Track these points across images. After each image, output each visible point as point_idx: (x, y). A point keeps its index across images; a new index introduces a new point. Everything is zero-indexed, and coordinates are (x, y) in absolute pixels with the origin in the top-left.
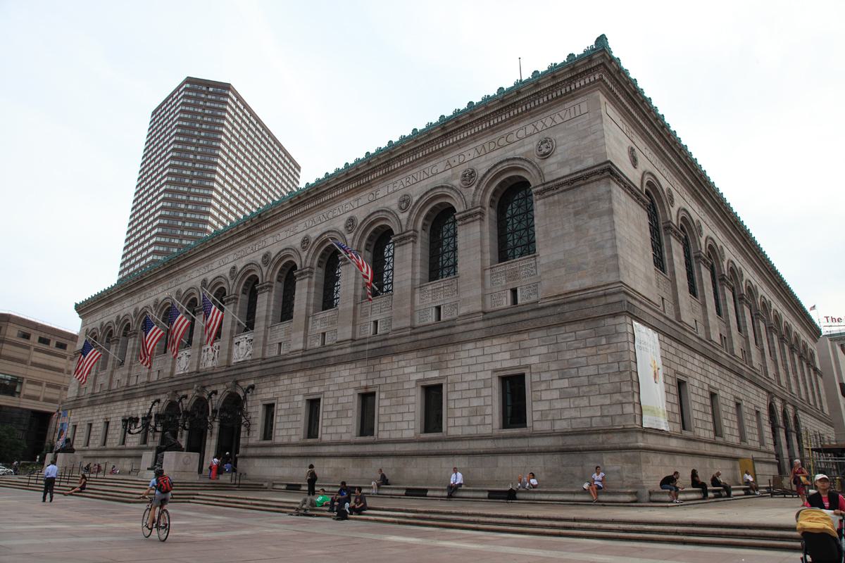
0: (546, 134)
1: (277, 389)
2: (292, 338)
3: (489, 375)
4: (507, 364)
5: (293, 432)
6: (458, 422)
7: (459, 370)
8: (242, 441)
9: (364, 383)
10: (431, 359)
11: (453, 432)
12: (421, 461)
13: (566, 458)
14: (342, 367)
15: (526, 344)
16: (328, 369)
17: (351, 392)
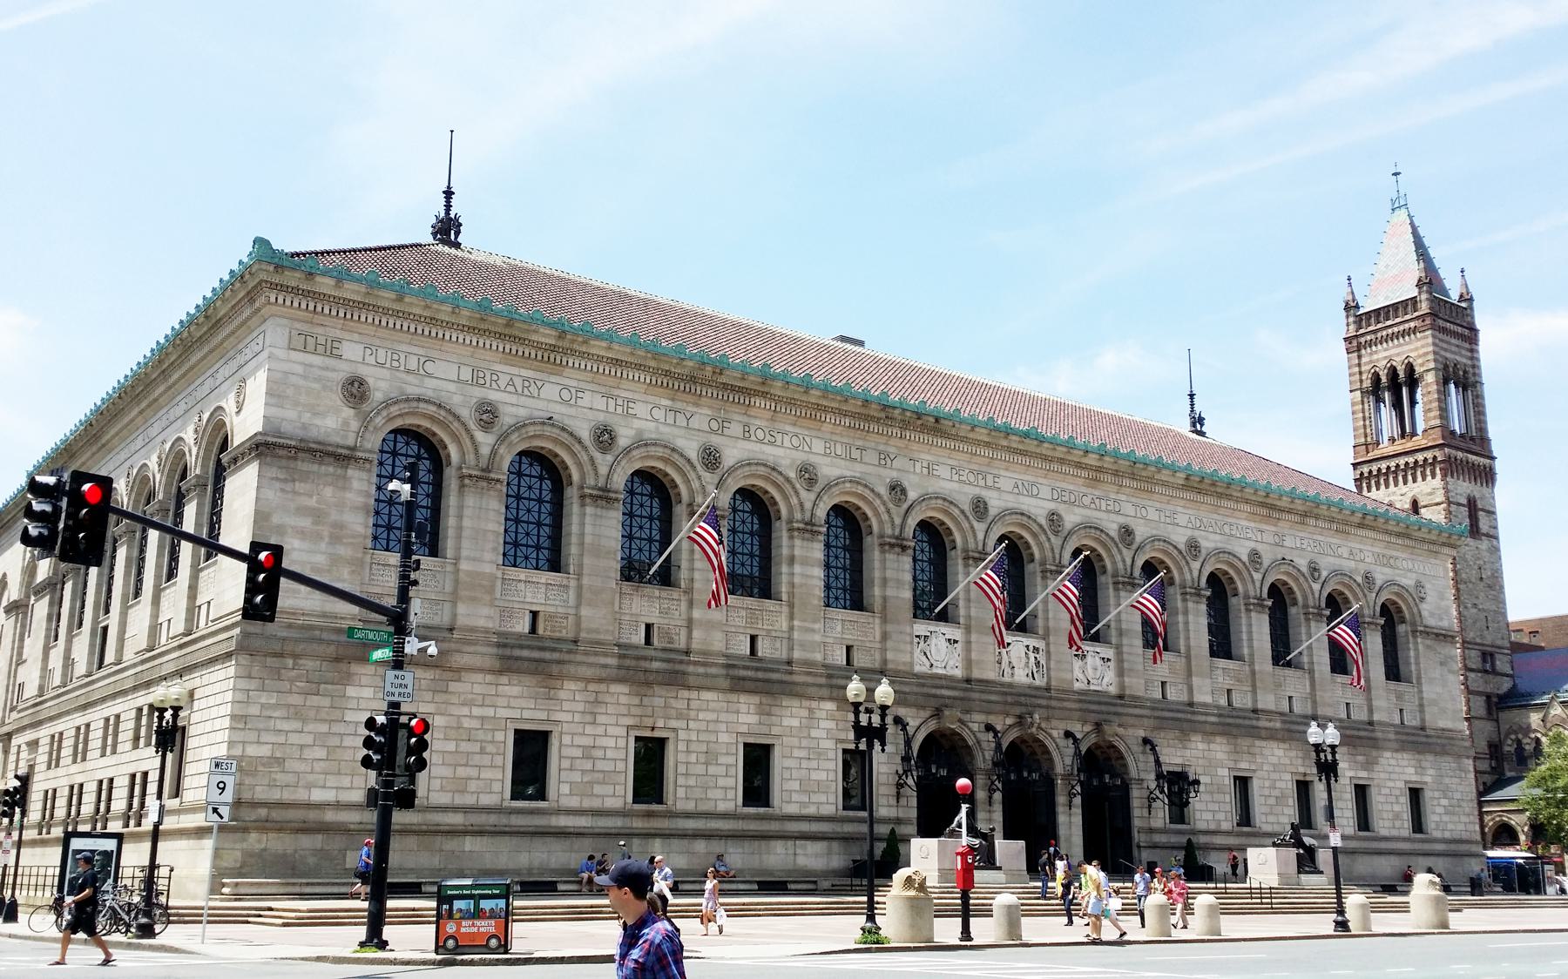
0: (1422, 579)
1: (1188, 753)
2: (1211, 684)
3: (1402, 785)
4: (1414, 778)
5: (1221, 816)
6: (1387, 824)
7: (1382, 776)
8: (1137, 823)
9: (1301, 770)
10: (1360, 758)
11: (1384, 832)
12: (1367, 858)
13: (1455, 860)
14: (1274, 744)
15: (1424, 764)
16: (1258, 743)
17: (1288, 777)
